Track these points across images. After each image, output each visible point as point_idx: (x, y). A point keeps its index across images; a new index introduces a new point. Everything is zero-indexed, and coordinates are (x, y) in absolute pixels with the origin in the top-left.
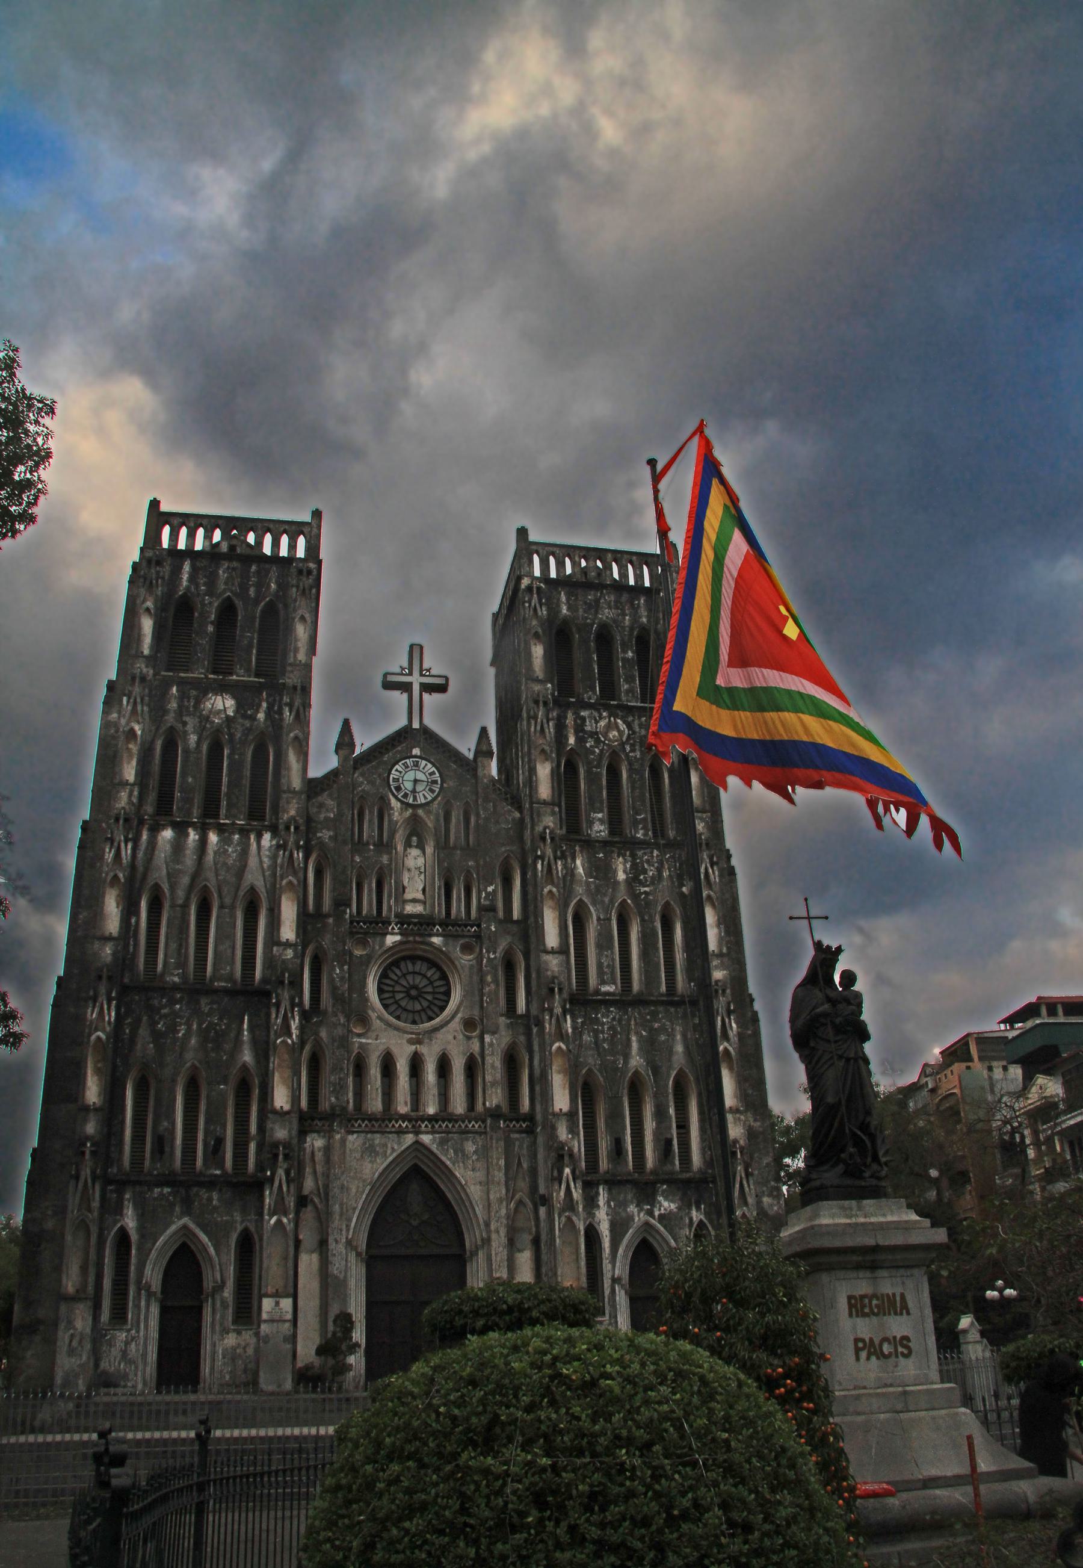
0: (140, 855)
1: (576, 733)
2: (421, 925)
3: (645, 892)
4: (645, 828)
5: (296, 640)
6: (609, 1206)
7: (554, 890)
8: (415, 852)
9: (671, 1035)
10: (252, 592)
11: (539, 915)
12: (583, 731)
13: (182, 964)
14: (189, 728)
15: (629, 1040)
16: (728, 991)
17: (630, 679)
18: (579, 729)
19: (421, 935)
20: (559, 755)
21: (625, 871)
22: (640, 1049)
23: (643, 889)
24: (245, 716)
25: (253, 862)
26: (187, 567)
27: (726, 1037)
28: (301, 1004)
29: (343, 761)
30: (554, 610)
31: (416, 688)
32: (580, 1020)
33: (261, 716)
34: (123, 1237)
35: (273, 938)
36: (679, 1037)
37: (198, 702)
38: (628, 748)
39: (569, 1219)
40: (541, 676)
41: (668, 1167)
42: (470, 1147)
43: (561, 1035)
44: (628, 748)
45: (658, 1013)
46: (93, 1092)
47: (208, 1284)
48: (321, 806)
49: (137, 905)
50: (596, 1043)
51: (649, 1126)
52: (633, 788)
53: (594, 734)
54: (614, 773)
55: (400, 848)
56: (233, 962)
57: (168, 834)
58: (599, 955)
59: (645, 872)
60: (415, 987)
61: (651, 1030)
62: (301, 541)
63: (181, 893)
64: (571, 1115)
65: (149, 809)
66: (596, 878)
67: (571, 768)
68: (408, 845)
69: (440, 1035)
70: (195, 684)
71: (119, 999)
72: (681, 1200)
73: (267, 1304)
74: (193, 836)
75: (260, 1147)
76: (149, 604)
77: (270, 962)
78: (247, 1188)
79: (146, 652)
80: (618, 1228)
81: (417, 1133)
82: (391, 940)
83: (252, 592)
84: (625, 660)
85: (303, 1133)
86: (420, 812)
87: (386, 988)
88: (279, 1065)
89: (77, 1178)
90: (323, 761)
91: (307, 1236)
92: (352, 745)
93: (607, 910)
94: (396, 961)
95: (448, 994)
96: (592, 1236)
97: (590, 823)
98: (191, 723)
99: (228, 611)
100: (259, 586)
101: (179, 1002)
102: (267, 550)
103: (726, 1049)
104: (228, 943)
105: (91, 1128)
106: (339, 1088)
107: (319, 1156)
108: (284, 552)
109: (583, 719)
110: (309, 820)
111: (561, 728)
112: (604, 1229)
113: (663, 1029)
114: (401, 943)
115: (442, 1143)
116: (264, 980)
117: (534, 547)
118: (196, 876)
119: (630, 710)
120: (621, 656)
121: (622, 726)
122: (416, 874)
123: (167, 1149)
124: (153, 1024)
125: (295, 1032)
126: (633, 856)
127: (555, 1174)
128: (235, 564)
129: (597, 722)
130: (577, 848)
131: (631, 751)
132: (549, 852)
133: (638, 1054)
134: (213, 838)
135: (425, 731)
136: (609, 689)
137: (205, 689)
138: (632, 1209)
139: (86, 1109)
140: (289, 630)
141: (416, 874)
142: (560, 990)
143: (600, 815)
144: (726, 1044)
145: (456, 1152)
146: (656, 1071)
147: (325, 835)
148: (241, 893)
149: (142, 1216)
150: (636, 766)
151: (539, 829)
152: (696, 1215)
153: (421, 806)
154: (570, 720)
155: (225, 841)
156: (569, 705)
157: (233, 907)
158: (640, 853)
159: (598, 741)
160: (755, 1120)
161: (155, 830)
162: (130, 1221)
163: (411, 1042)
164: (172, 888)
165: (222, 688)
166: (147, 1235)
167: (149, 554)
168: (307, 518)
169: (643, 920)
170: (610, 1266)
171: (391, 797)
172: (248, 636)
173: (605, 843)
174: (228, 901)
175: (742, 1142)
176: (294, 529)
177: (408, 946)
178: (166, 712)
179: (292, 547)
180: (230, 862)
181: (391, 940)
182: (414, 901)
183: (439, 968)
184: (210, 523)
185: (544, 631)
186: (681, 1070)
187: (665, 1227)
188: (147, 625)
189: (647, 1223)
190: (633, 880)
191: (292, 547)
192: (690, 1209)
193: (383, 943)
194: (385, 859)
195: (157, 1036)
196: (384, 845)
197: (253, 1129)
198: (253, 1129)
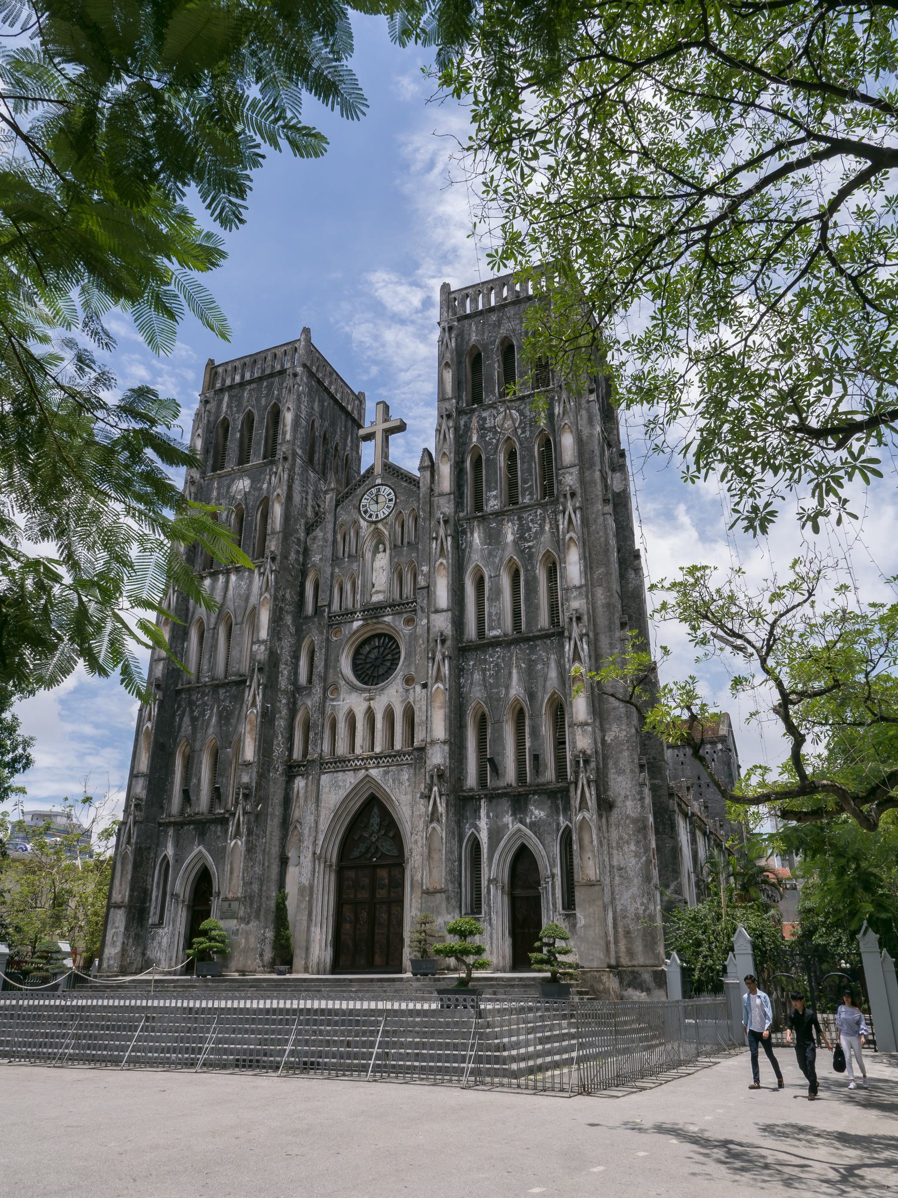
3: (529, 547)
4: (531, 494)
5: (284, 426)
6: (488, 817)
7: (444, 562)
9: (547, 664)
10: (263, 401)
15: (510, 673)
16: (585, 618)
18: (482, 428)
19: (377, 617)
22: (519, 680)
23: (527, 545)
24: (255, 489)
26: (226, 399)
27: (577, 657)
31: (379, 436)
33: (265, 486)
36: (553, 665)
37: (229, 487)
38: (519, 431)
41: (542, 780)
44: (519, 431)
45: (537, 646)
50: (484, 680)
52: (523, 463)
55: (368, 555)
58: (490, 606)
59: (530, 529)
60: (377, 658)
61: (530, 660)
64: (444, 742)
66: (489, 544)
69: (386, 692)
70: (229, 474)
74: (221, 578)
76: (200, 431)
80: (495, 835)
81: (367, 769)
82: (356, 624)
83: (263, 401)
86: (380, 526)
87: (358, 662)
88: (251, 730)
91: (291, 854)
93: (498, 569)
96: (476, 845)
97: (488, 500)
100: (267, 395)
101: (207, 695)
104: (238, 649)
109: (484, 419)
112: (484, 837)
114: (363, 625)
115: (386, 773)
117: (453, 296)
122: (379, 572)
123: (193, 798)
124: (192, 711)
125: (259, 703)
126: (520, 519)
128: (254, 386)
129: (495, 418)
131: (523, 432)
132: (442, 532)
133: (518, 684)
134: (233, 578)
137: (233, 477)
138: (508, 819)
141: (379, 572)
142: (443, 642)
143: (494, 493)
145: (394, 782)
146: (532, 695)
148: (248, 612)
149: (177, 845)
150: (526, 444)
152: (563, 822)
154: (474, 424)
155: (240, 578)
157: (242, 623)
158: (525, 515)
159: (496, 432)
162: (170, 851)
163: (365, 700)
165: (242, 473)
166: (179, 860)
168: (296, 334)
169: (526, 570)
170: (486, 869)
171: (362, 521)
172: (260, 432)
173: (497, 514)
174: (239, 619)
175: (589, 752)
176: (291, 347)
177: (369, 628)
180: (242, 592)
181: (356, 624)
182: (377, 592)
185: (452, 359)
186: (554, 693)
187: (535, 833)
189: (519, 830)
190: (521, 537)
192: (558, 813)
193: (351, 628)
194: (355, 566)
195: (194, 720)
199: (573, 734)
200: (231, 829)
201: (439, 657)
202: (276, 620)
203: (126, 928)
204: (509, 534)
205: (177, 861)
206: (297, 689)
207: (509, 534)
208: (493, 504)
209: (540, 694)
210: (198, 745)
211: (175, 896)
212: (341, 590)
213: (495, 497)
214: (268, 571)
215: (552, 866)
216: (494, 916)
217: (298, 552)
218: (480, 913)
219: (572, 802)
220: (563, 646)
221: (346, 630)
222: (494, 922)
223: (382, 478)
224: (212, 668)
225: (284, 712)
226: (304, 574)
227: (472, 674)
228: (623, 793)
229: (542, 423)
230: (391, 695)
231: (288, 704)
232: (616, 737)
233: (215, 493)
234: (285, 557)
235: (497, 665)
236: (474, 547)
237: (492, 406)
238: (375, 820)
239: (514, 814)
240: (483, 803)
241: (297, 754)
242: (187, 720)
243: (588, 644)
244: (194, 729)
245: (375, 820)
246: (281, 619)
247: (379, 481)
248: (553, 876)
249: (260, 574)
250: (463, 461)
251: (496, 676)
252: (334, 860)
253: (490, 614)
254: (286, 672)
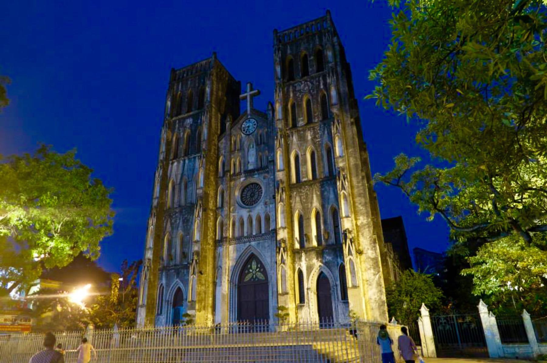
1: (293, 92)
6: (306, 260)
9: (329, 192)
12: (295, 91)
15: (312, 197)
21: (311, 136)
22: (318, 199)
32: (295, 193)
33: (199, 121)
36: (332, 192)
37: (183, 122)
39: (282, 267)
40: (280, 77)
42: (266, 245)
50: (301, 200)
51: (322, 227)
53: (299, 91)
55: (246, 150)
56: (192, 198)
63: (178, 181)
72: (334, 255)
79: (169, 113)
80: (310, 269)
81: (250, 242)
82: (242, 179)
84: (310, 61)
97: (299, 122)
103: (344, 193)
113: (326, 190)
119: (312, 78)
120: (309, 59)
127: (278, 250)
130: (294, 131)
131: (313, 91)
134: (187, 161)
136: (305, 73)
143: (302, 118)
144: (343, 191)
146: (323, 206)
153: (251, 133)
160: (364, 219)
161: (172, 163)
164: (176, 180)
166: (168, 285)
178: (175, 128)
192: (337, 257)
195: (171, 224)
199: (343, 221)
200: (191, 271)
202: (207, 177)
203: (146, 316)
205: (167, 286)
208: (301, 122)
209: (326, 206)
213: (302, 120)
215: (336, 280)
216: (310, 304)
217: (215, 149)
218: (304, 303)
219: (344, 252)
220: (336, 184)
221: (238, 182)
222: (311, 307)
223: (251, 115)
224: (180, 201)
225: (212, 219)
226: (218, 159)
227: (295, 198)
228: (366, 248)
229: (322, 87)
230: (259, 209)
231: (213, 216)
232: (362, 223)
233: (177, 126)
234: (210, 150)
235: (307, 194)
236: (294, 142)
238: (254, 266)
239: (317, 259)
240: (303, 255)
243: (348, 182)
244: (172, 228)
245: (254, 266)
246: (209, 178)
247: (249, 117)
248: (336, 286)
249: (199, 159)
250: (287, 105)
251: (307, 198)
252: (237, 283)
253: (302, 171)
254: (212, 202)
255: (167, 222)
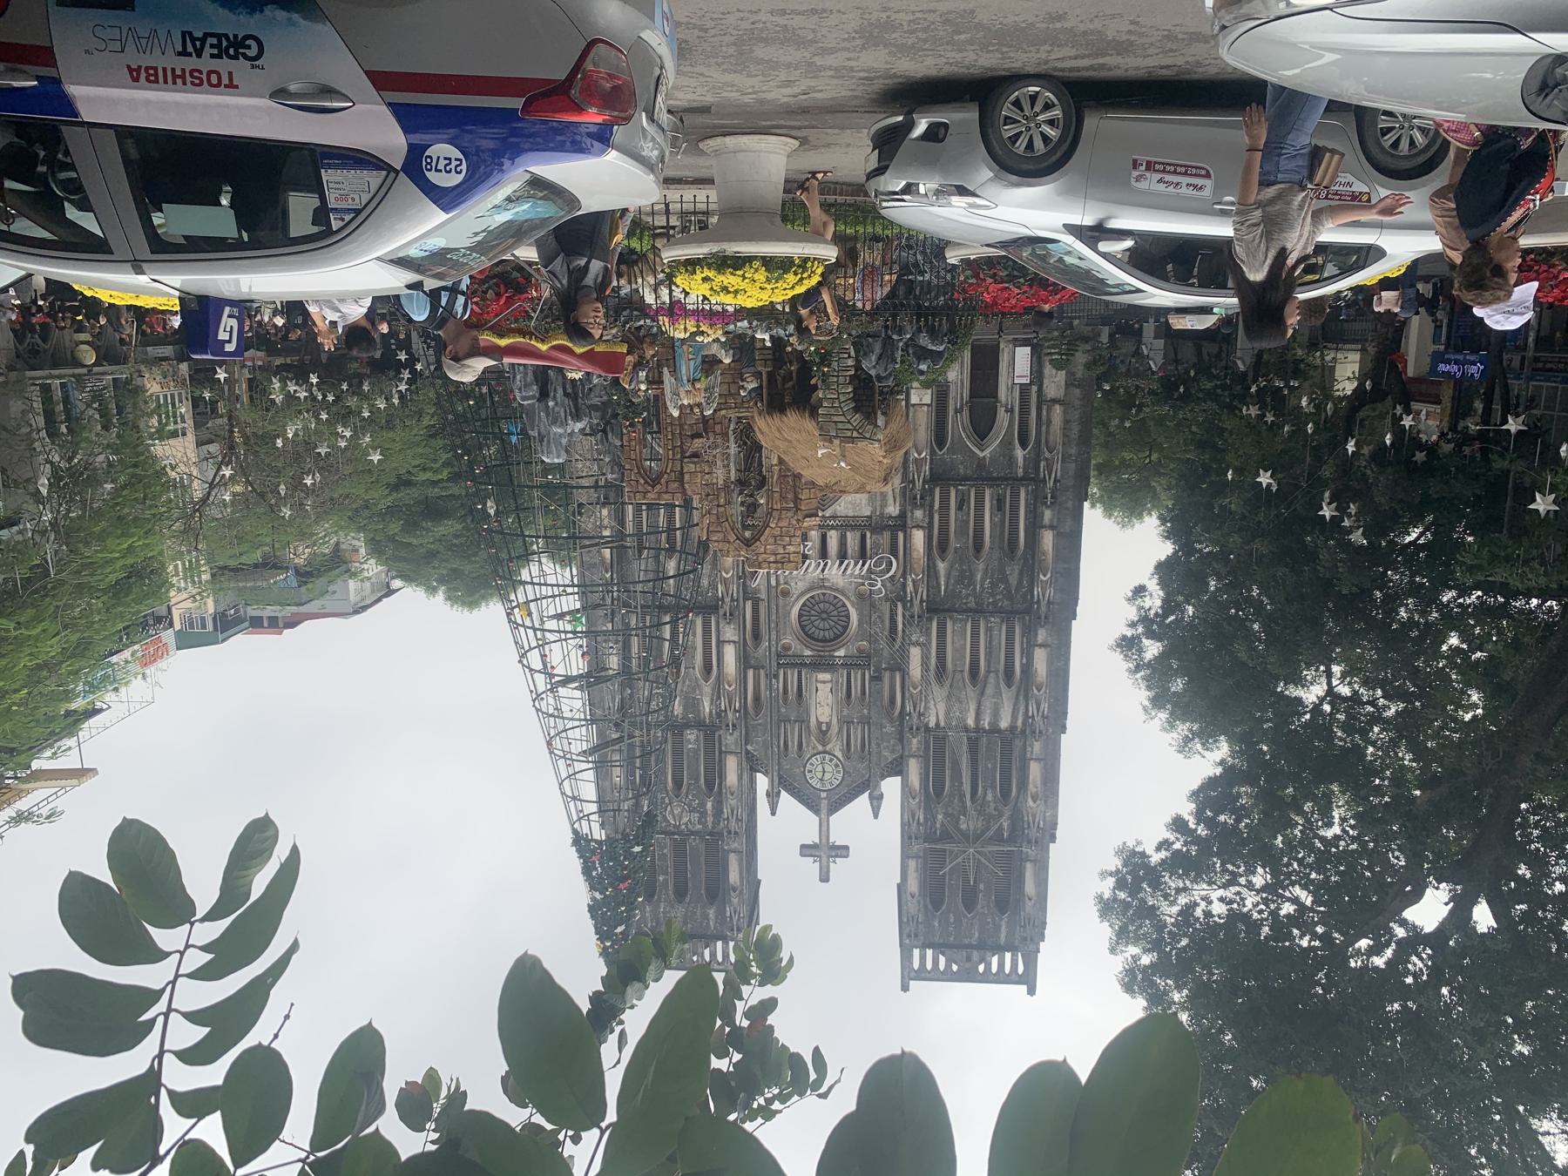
0: (1022, 709)
2: (822, 664)
8: (824, 719)
11: (738, 668)
13: (989, 630)
14: (992, 806)
17: (663, 857)
18: (703, 814)
20: (720, 792)
24: (952, 815)
25: (942, 707)
28: (904, 607)
29: (877, 786)
30: (721, 913)
34: (1024, 445)
35: (925, 647)
40: (733, 858)
43: (725, 582)
46: (1048, 539)
47: (966, 413)
48: (893, 751)
49: (1022, 672)
54: (678, 784)
55: (835, 721)
57: (1004, 724)
62: (916, 965)
63: (992, 680)
65: (1018, 743)
67: (710, 785)
68: (829, 724)
71: (1032, 602)
73: (927, 399)
75: (932, 506)
77: (928, 633)
78: (940, 477)
79: (1029, 866)
82: (841, 653)
85: (902, 515)
86: (820, 748)
89: (1056, 481)
90: (891, 787)
92: (871, 798)
94: (838, 638)
95: (800, 615)
97: (697, 740)
98: (991, 809)
99: (970, 903)
102: (942, 959)
105: (1048, 514)
106: (876, 546)
107: (891, 501)
108: (929, 953)
110: (901, 740)
111: (718, 812)
116: (930, 620)
118: (982, 694)
121: (670, 818)
122: (823, 700)
125: (910, 583)
128: (966, 941)
132: (730, 715)
134: (971, 722)
135: (815, 810)
136: (679, 850)
139: (1052, 527)
140: (923, 884)
141: (823, 700)
147: (889, 729)
148: (948, 683)
149: (1012, 459)
151: (736, 734)
154: (710, 819)
156: (711, 834)
161: (1012, 728)
162: (1019, 453)
166: (1007, 444)
167: (1032, 947)
173: (687, 726)
174: (958, 676)
176: (922, 975)
178: (1011, 818)
179: (923, 958)
181: (841, 653)
183: (807, 634)
184: (987, 978)
188: (1030, 888)
191: (923, 958)
194: (845, 712)
195: (1004, 580)
196: (846, 722)
197: (936, 517)
198: (936, 517)
201: (727, 600)
204: (677, 708)
205: (1011, 443)
206: (903, 599)
207: (677, 708)
210: (996, 555)
211: (1010, 411)
212: (863, 693)
214: (915, 716)
237: (692, 833)
241: (901, 535)
242: (1013, 580)
244: (1002, 571)
247: (824, 795)
255: (1017, 590)
